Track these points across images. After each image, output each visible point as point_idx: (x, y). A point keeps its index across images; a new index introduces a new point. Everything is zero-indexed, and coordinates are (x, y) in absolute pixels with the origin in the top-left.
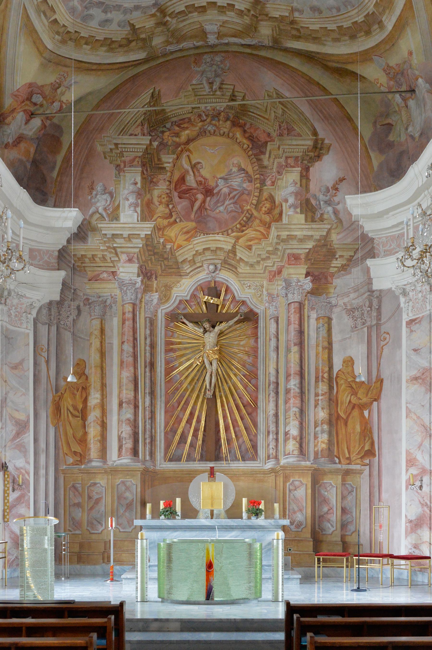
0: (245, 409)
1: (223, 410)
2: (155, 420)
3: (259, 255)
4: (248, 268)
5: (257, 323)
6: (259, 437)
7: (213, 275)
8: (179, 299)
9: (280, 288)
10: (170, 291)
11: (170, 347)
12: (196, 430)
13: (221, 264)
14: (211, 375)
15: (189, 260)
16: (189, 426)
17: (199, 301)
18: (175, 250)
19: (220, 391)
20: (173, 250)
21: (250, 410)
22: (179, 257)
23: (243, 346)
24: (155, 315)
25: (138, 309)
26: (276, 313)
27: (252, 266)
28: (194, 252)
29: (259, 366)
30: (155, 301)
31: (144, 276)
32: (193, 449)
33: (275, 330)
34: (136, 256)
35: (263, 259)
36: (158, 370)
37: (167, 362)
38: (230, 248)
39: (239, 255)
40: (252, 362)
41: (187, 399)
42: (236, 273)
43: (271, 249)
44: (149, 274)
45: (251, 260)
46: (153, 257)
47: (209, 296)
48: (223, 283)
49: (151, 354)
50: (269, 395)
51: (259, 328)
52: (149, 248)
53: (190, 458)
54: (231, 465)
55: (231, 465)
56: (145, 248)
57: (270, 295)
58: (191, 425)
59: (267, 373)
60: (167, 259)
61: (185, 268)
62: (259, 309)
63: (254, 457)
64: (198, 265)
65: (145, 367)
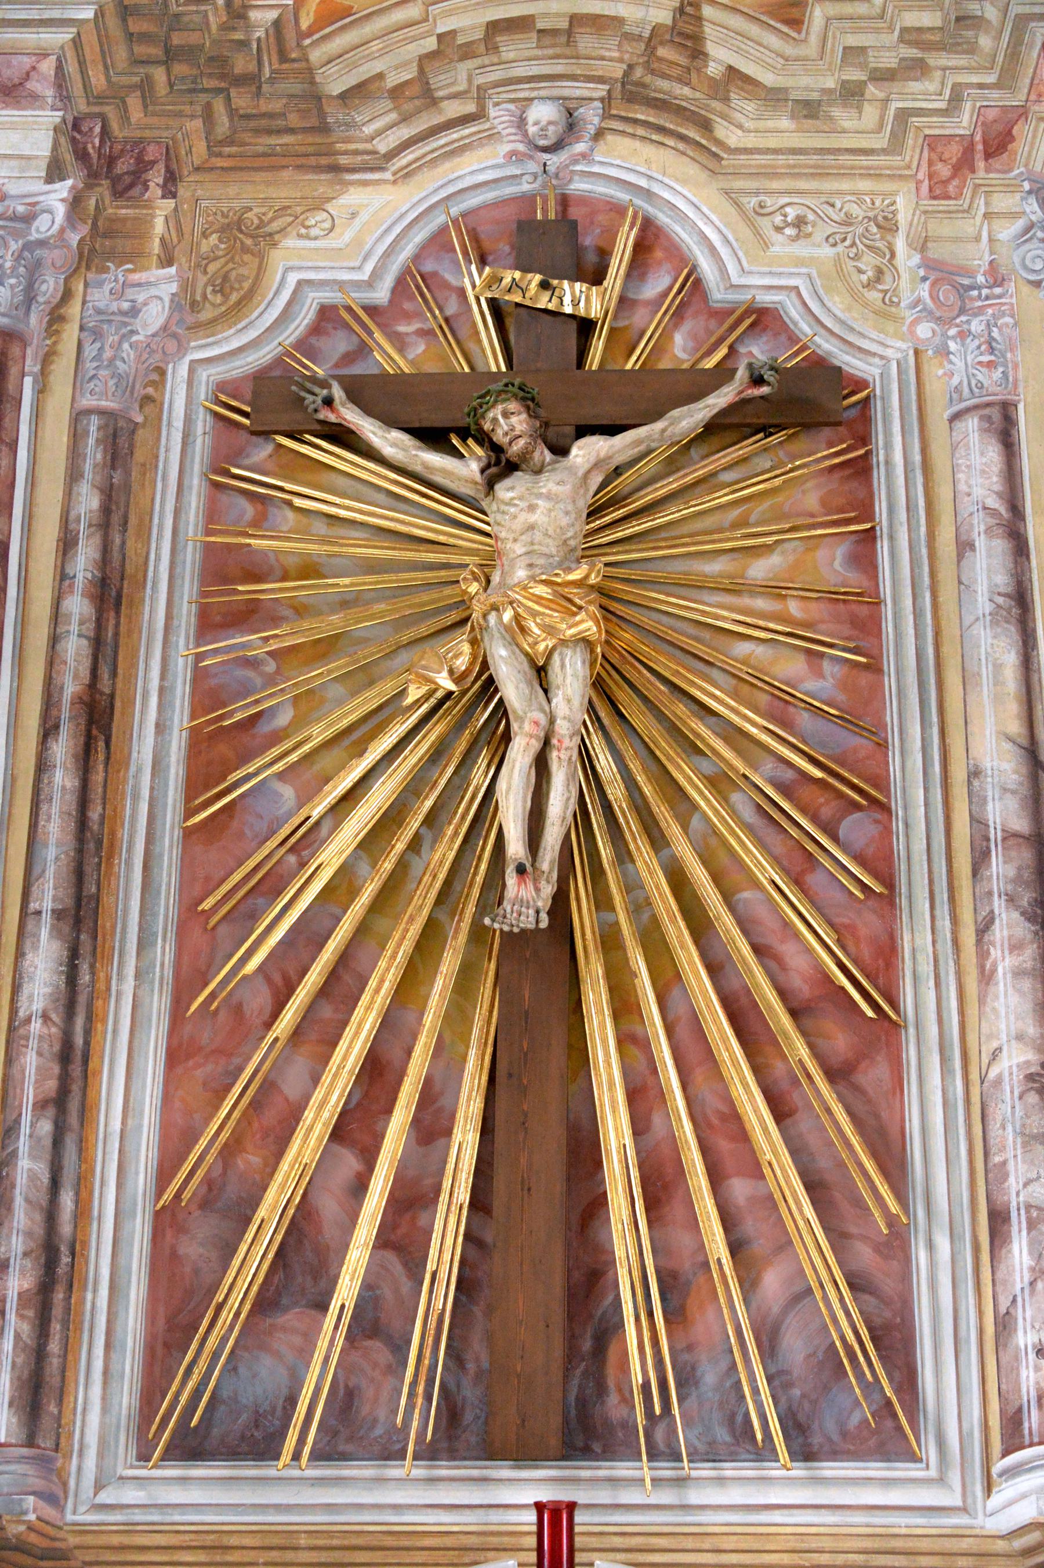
0: (804, 1033)
1: (631, 1041)
2: (87, 1112)
3: (853, 54)
4: (785, 123)
5: (864, 439)
6: (921, 1256)
7: (554, 161)
8: (313, 300)
9: (1007, 231)
10: (261, 256)
11: (233, 592)
12: (412, 1200)
13: (607, 101)
14: (541, 764)
15: (391, 82)
16: (350, 1162)
17: (452, 307)
18: (302, 36)
19: (602, 902)
20: (290, 36)
21: (841, 1042)
22: (333, 69)
23: (774, 590)
24: (147, 400)
25: (32, 365)
26: (990, 379)
27: (809, 110)
28: (431, 44)
29: (891, 717)
30: (154, 316)
31: (93, 177)
32: (380, 1351)
33: (995, 481)
34: (47, 67)
35: (883, 76)
36: (143, 749)
37: (208, 694)
38: (663, 16)
39: (720, 55)
40: (841, 697)
41: (344, 958)
42: (710, 155)
43: (928, 19)
44: (122, 167)
45: (805, 81)
46: (159, 75)
47: (525, 270)
48: (619, 210)
49: (97, 643)
50: (984, 929)
51: (879, 477)
52: (136, 26)
53: (350, 1433)
54: (695, 1496)
55: (695, 1496)
56: (112, 23)
57: (940, 273)
58: (369, 1157)
59: (959, 774)
60: (251, 80)
61: (368, 130)
62: (874, 353)
63: (890, 1432)
64: (453, 109)
65: (48, 730)
